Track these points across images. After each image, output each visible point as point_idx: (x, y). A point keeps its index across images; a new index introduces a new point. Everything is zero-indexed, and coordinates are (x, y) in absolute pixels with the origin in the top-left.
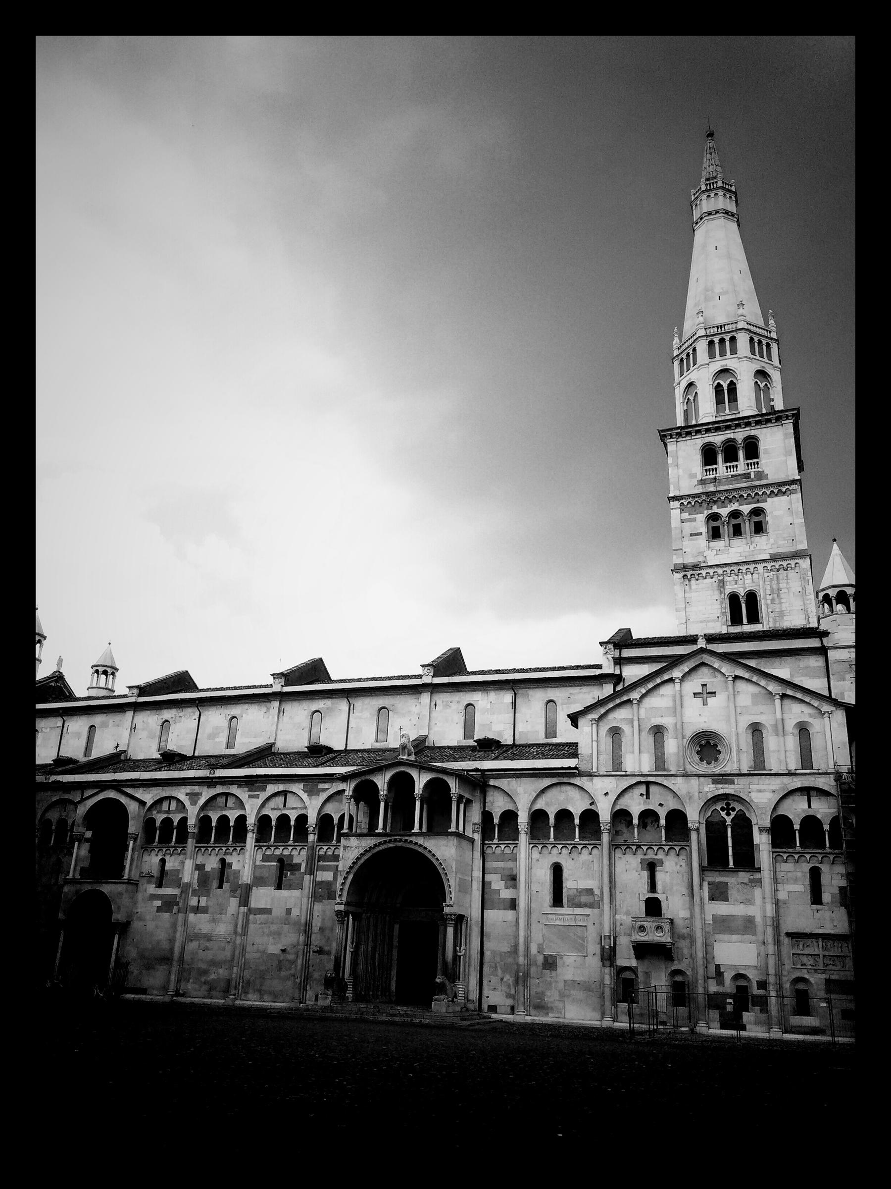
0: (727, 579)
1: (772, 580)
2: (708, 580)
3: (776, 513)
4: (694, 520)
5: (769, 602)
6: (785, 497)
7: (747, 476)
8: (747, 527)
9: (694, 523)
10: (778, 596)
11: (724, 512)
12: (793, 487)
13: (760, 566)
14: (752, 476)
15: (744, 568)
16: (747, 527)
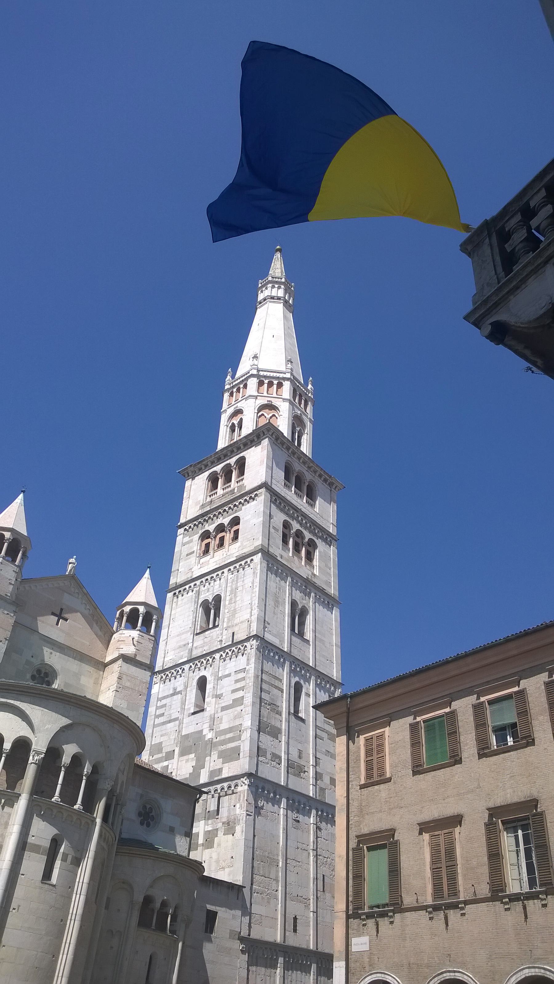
0: (202, 588)
1: (233, 581)
2: (190, 593)
3: (245, 519)
4: (191, 541)
5: (227, 603)
6: (255, 501)
7: (232, 491)
8: (228, 537)
9: (191, 544)
10: (235, 595)
11: (211, 527)
12: (260, 491)
13: (226, 570)
14: (236, 491)
15: (214, 575)
16: (228, 537)
